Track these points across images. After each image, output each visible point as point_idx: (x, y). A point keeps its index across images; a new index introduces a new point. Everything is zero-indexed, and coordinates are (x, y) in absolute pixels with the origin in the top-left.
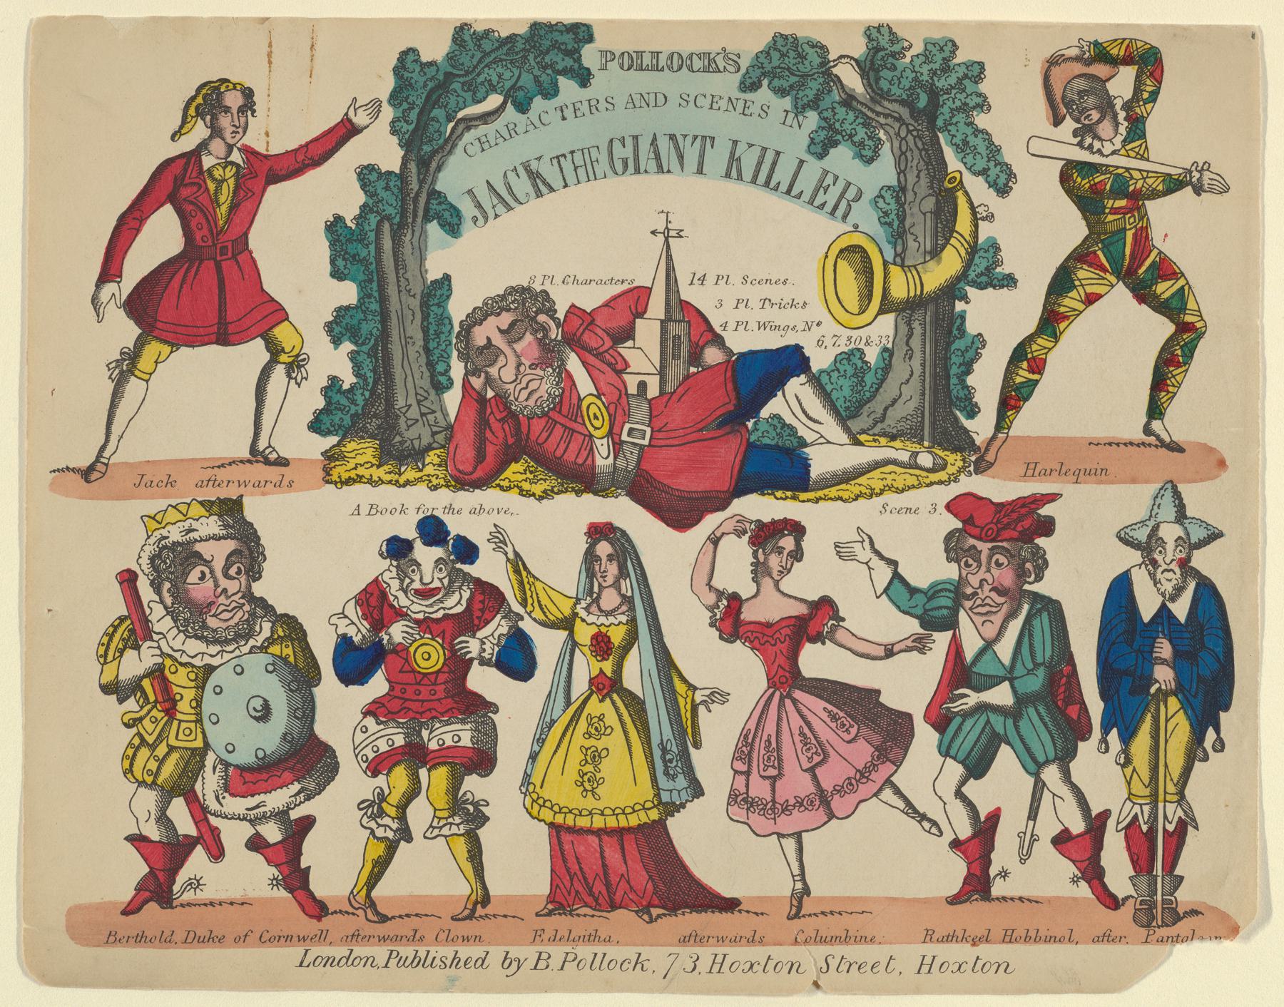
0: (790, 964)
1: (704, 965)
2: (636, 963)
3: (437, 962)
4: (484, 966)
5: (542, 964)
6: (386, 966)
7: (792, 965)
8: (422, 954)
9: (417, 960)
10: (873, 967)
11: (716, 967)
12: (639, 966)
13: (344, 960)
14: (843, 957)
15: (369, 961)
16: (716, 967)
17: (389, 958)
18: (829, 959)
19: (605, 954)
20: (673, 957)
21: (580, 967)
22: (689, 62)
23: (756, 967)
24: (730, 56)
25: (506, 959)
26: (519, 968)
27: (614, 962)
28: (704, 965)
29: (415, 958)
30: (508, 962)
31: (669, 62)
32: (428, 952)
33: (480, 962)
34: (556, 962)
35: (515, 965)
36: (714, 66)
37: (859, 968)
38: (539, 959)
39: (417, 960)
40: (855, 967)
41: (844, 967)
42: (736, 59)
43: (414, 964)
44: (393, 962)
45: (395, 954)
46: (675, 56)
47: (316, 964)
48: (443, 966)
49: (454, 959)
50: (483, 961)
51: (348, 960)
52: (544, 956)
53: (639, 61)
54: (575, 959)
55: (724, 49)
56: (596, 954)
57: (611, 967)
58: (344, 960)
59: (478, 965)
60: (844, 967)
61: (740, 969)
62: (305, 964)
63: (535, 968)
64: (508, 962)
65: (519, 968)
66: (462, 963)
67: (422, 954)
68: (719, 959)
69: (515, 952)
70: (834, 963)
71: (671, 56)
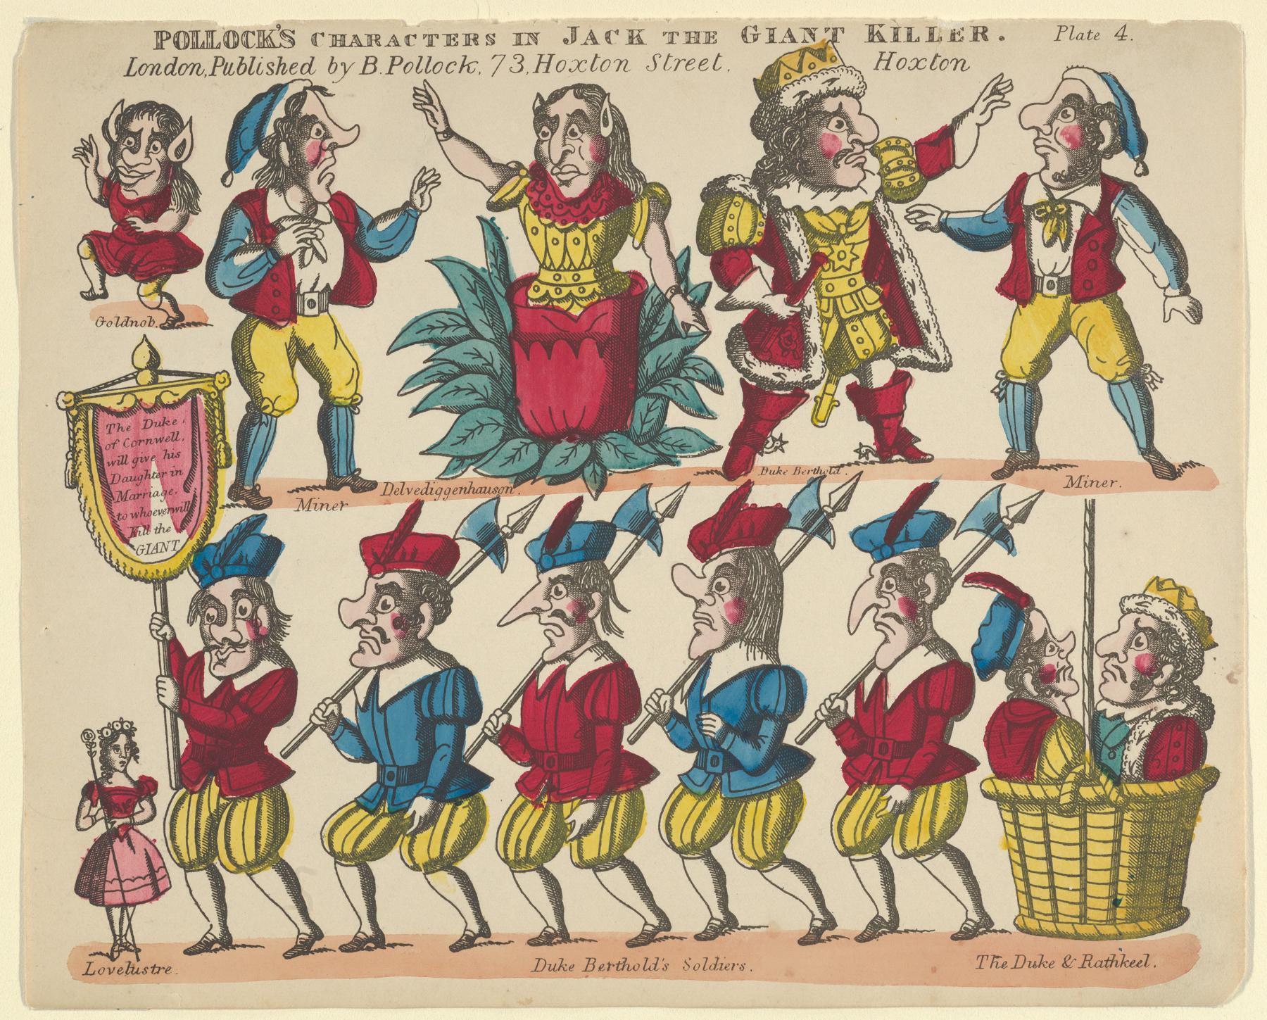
2: (463, 66)
3: (264, 68)
5: (370, 68)
6: (213, 74)
7: (621, 62)
8: (248, 61)
9: (242, 68)
10: (700, 65)
11: (543, 67)
12: (466, 68)
13: (171, 67)
14: (669, 56)
15: (195, 68)
17: (215, 66)
18: (656, 58)
20: (498, 59)
23: (582, 67)
25: (332, 63)
26: (346, 72)
30: (334, 66)
32: (254, 58)
33: (306, 67)
34: (383, 65)
35: (341, 69)
37: (688, 64)
38: (366, 63)
39: (242, 68)
40: (683, 64)
41: (672, 63)
44: (219, 71)
45: (220, 62)
47: (142, 72)
49: (280, 65)
50: (310, 66)
51: (174, 65)
52: (371, 60)
54: (402, 60)
56: (421, 57)
57: (436, 70)
58: (171, 67)
60: (672, 63)
62: (131, 73)
63: (363, 73)
64: (334, 66)
65: (346, 72)
66: (288, 67)
67: (248, 61)
70: (660, 62)
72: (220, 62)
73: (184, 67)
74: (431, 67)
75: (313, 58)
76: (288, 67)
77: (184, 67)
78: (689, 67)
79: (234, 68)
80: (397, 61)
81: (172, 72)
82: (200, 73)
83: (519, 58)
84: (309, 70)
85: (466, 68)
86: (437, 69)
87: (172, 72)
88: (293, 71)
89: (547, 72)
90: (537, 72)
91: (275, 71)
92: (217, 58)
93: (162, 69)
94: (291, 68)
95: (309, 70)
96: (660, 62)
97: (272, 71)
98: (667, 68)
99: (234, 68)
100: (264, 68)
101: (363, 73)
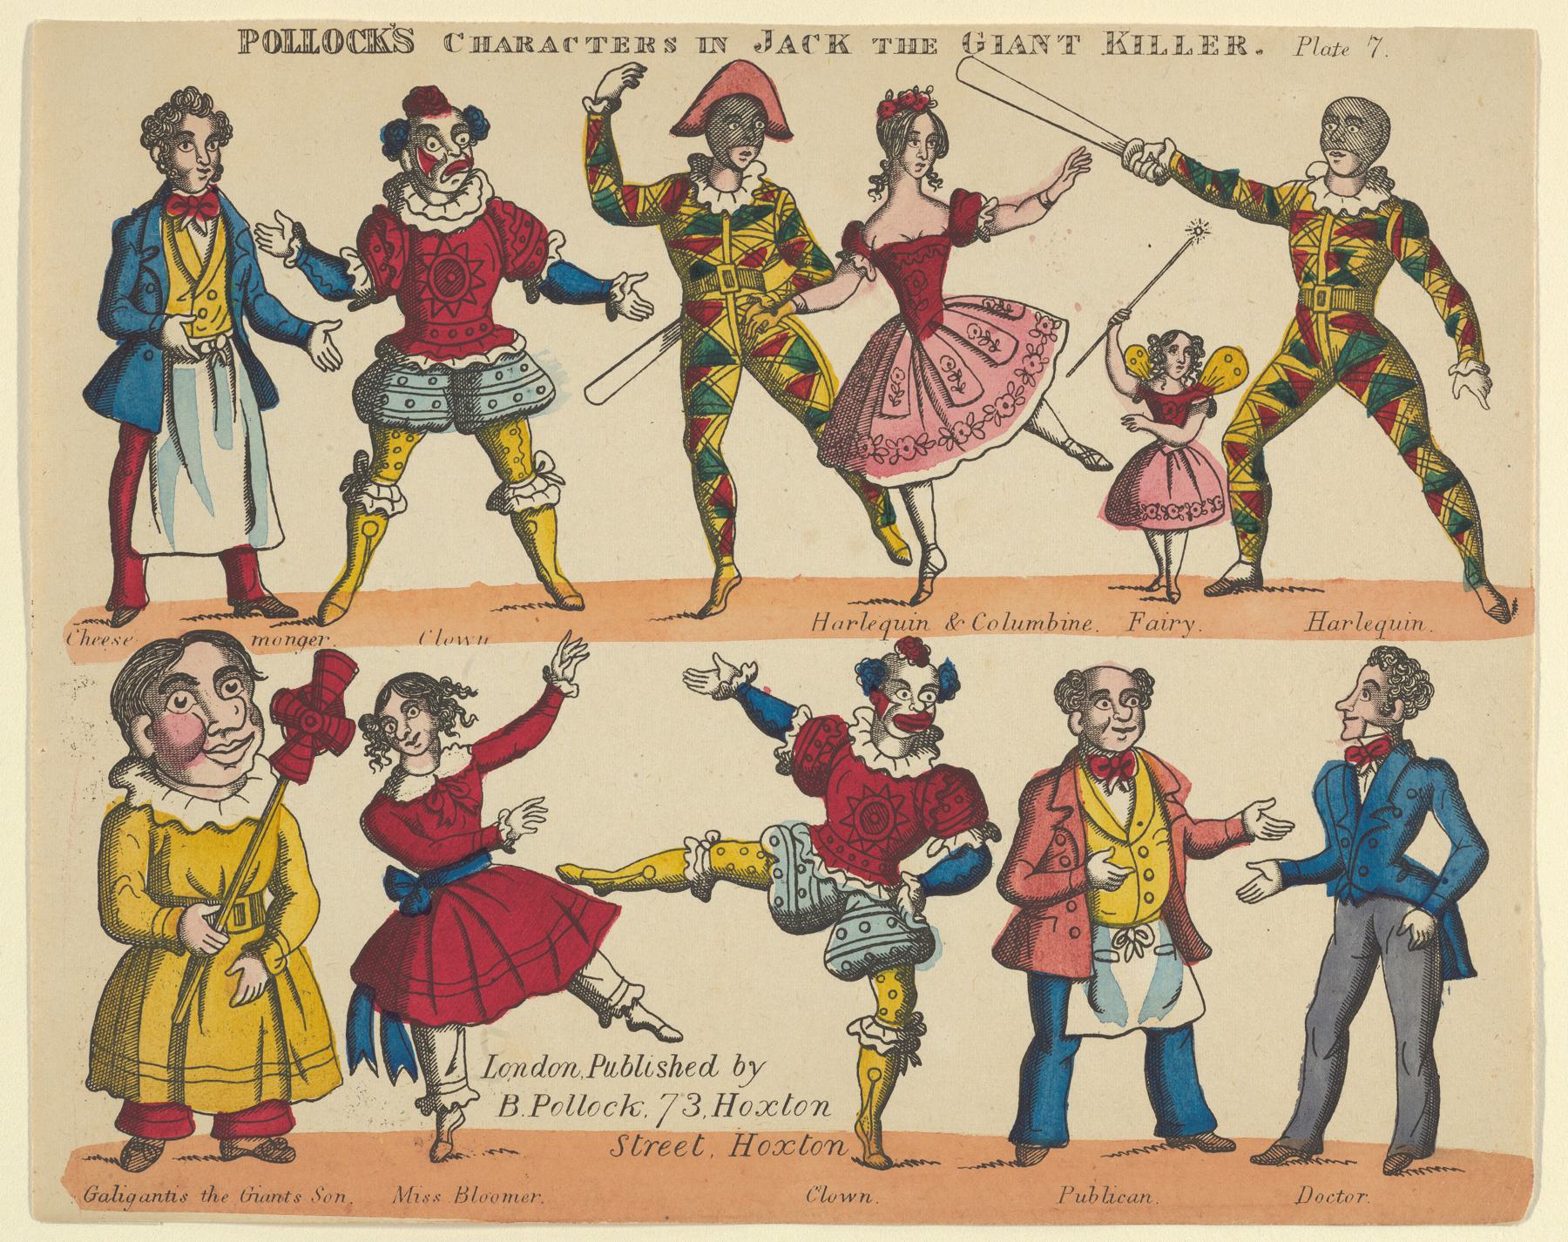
3: (654, 1068)
4: (713, 1073)
9: (628, 1068)
17: (594, 1065)
26: (755, 1073)
29: (626, 1063)
30: (740, 1066)
32: (642, 1056)
33: (707, 1067)
35: (749, 1069)
39: (628, 1068)
43: (625, 1073)
44: (599, 1071)
45: (599, 1062)
47: (503, 1073)
48: (662, 1074)
49: (674, 1065)
50: (711, 1066)
51: (543, 1066)
58: (539, 1067)
59: (703, 1073)
62: (491, 1074)
64: (740, 1067)
65: (755, 1073)
66: (684, 1068)
67: (634, 1060)
72: (599, 1062)
73: (556, 1067)
75: (715, 1056)
76: (684, 1068)
77: (556, 1067)
79: (618, 1069)
81: (540, 1073)
82: (575, 1074)
84: (710, 1071)
87: (540, 1073)
88: (690, 1072)
91: (668, 1073)
92: (597, 1056)
93: (529, 1069)
94: (687, 1069)
95: (710, 1071)
97: (665, 1073)
99: (618, 1069)
100: (654, 1068)
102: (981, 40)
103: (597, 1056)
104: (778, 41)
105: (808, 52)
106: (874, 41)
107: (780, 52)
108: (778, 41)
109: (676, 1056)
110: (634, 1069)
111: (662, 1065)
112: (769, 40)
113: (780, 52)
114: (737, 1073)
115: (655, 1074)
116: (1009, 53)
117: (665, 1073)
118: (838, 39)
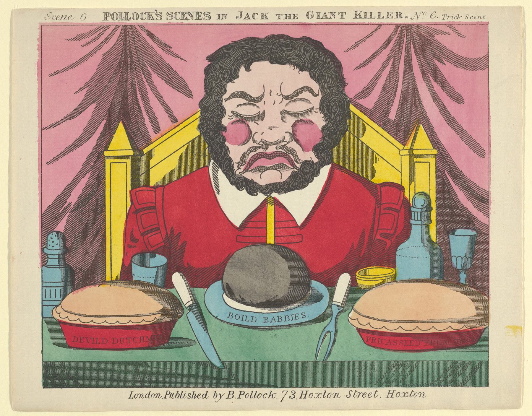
0: (334, 394)
1: (298, 395)
3: (187, 395)
4: (207, 397)
5: (231, 396)
6: (165, 398)
7: (336, 394)
8: (180, 393)
10: (368, 395)
11: (303, 396)
12: (271, 396)
15: (158, 395)
16: (303, 396)
17: (166, 394)
18: (350, 392)
19: (256, 392)
20: (285, 393)
21: (246, 397)
22: (141, 16)
24: (158, 13)
25: (215, 394)
26: (221, 398)
27: (260, 395)
28: (298, 395)
30: (216, 395)
31: (133, 16)
32: (183, 391)
34: (237, 394)
35: (219, 396)
36: (151, 17)
37: (363, 395)
38: (229, 394)
39: (178, 395)
40: (361, 395)
41: (357, 394)
42: (160, 14)
44: (168, 396)
45: (168, 393)
46: (135, 14)
47: (136, 397)
48: (189, 397)
49: (193, 394)
50: (206, 395)
51: (149, 395)
52: (231, 393)
53: (120, 17)
54: (244, 392)
55: (156, 10)
56: (253, 392)
57: (259, 397)
58: (148, 395)
60: (357, 394)
61: (313, 397)
62: (131, 397)
63: (228, 398)
64: (216, 395)
65: (221, 398)
66: (197, 395)
67: (180, 393)
68: (304, 393)
69: (219, 390)
70: (352, 394)
71: (133, 14)
72: (168, 393)
73: (153, 395)
74: (257, 395)
75: (207, 392)
76: (197, 395)
77: (153, 395)
78: (364, 396)
80: (242, 393)
81: (148, 397)
83: (294, 392)
84: (205, 397)
85: (271, 396)
86: (259, 397)
87: (148, 397)
88: (199, 397)
89: (305, 398)
90: (301, 398)
91: (191, 396)
92: (167, 391)
94: (198, 396)
95: (205, 397)
96: (352, 394)
97: (190, 397)
98: (355, 396)
100: (187, 395)
101: (228, 398)
102: (312, 14)
103: (167, 391)
104: (244, 15)
105: (254, 19)
106: (276, 15)
107: (245, 19)
108: (244, 15)
109: (194, 392)
110: (180, 396)
111: (189, 394)
112: (241, 15)
113: (245, 19)
114: (215, 397)
115: (187, 398)
116: (322, 18)
117: (190, 397)
118: (264, 14)
